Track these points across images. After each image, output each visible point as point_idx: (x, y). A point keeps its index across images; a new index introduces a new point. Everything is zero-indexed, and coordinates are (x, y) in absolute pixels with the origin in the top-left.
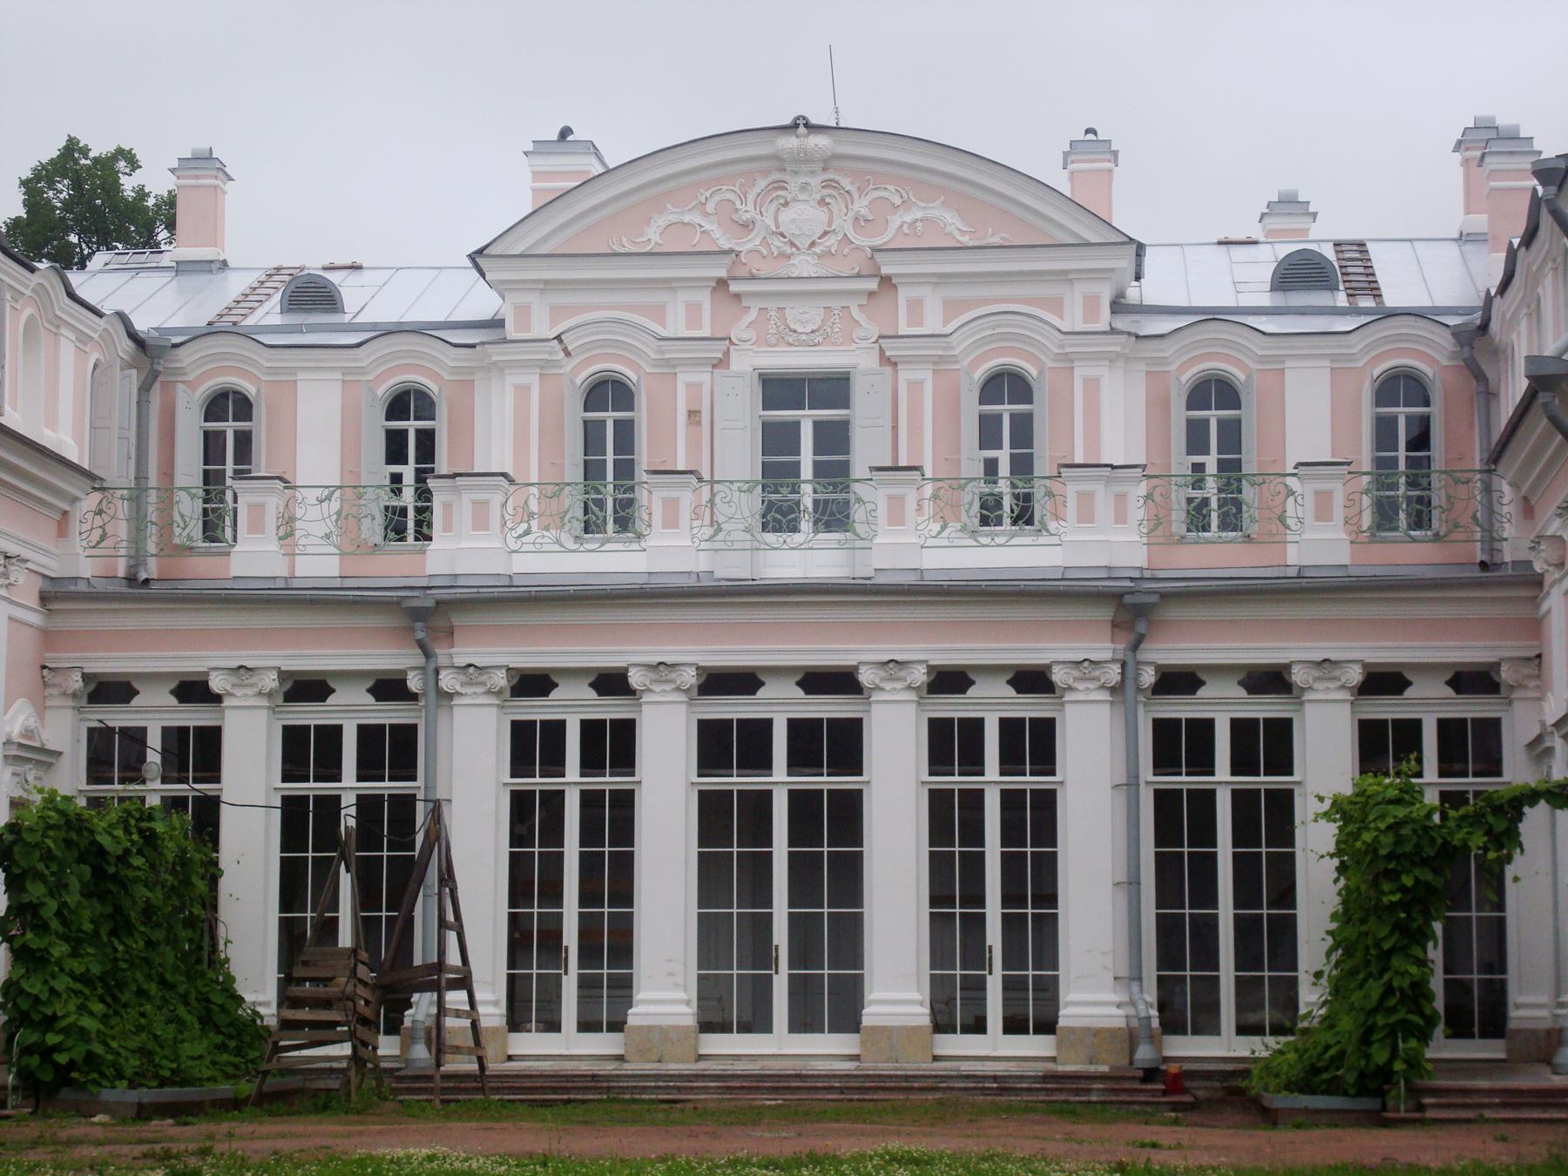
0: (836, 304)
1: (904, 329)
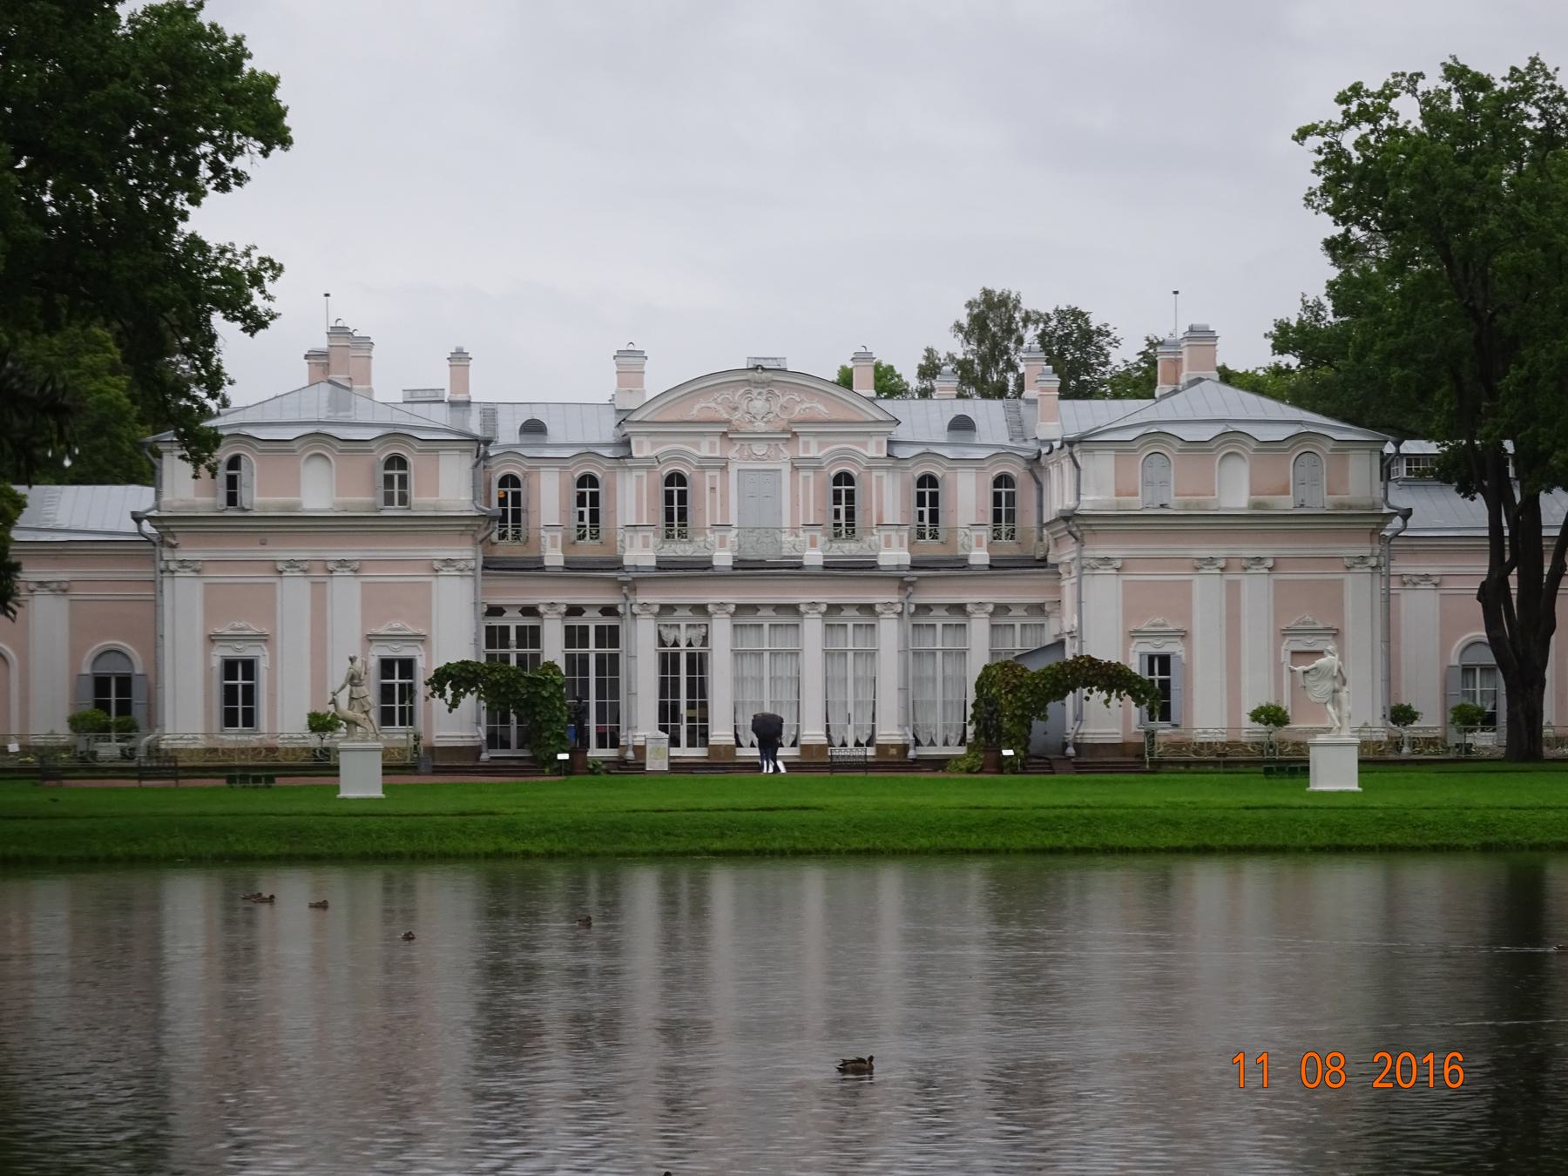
0: (772, 443)
1: (802, 455)
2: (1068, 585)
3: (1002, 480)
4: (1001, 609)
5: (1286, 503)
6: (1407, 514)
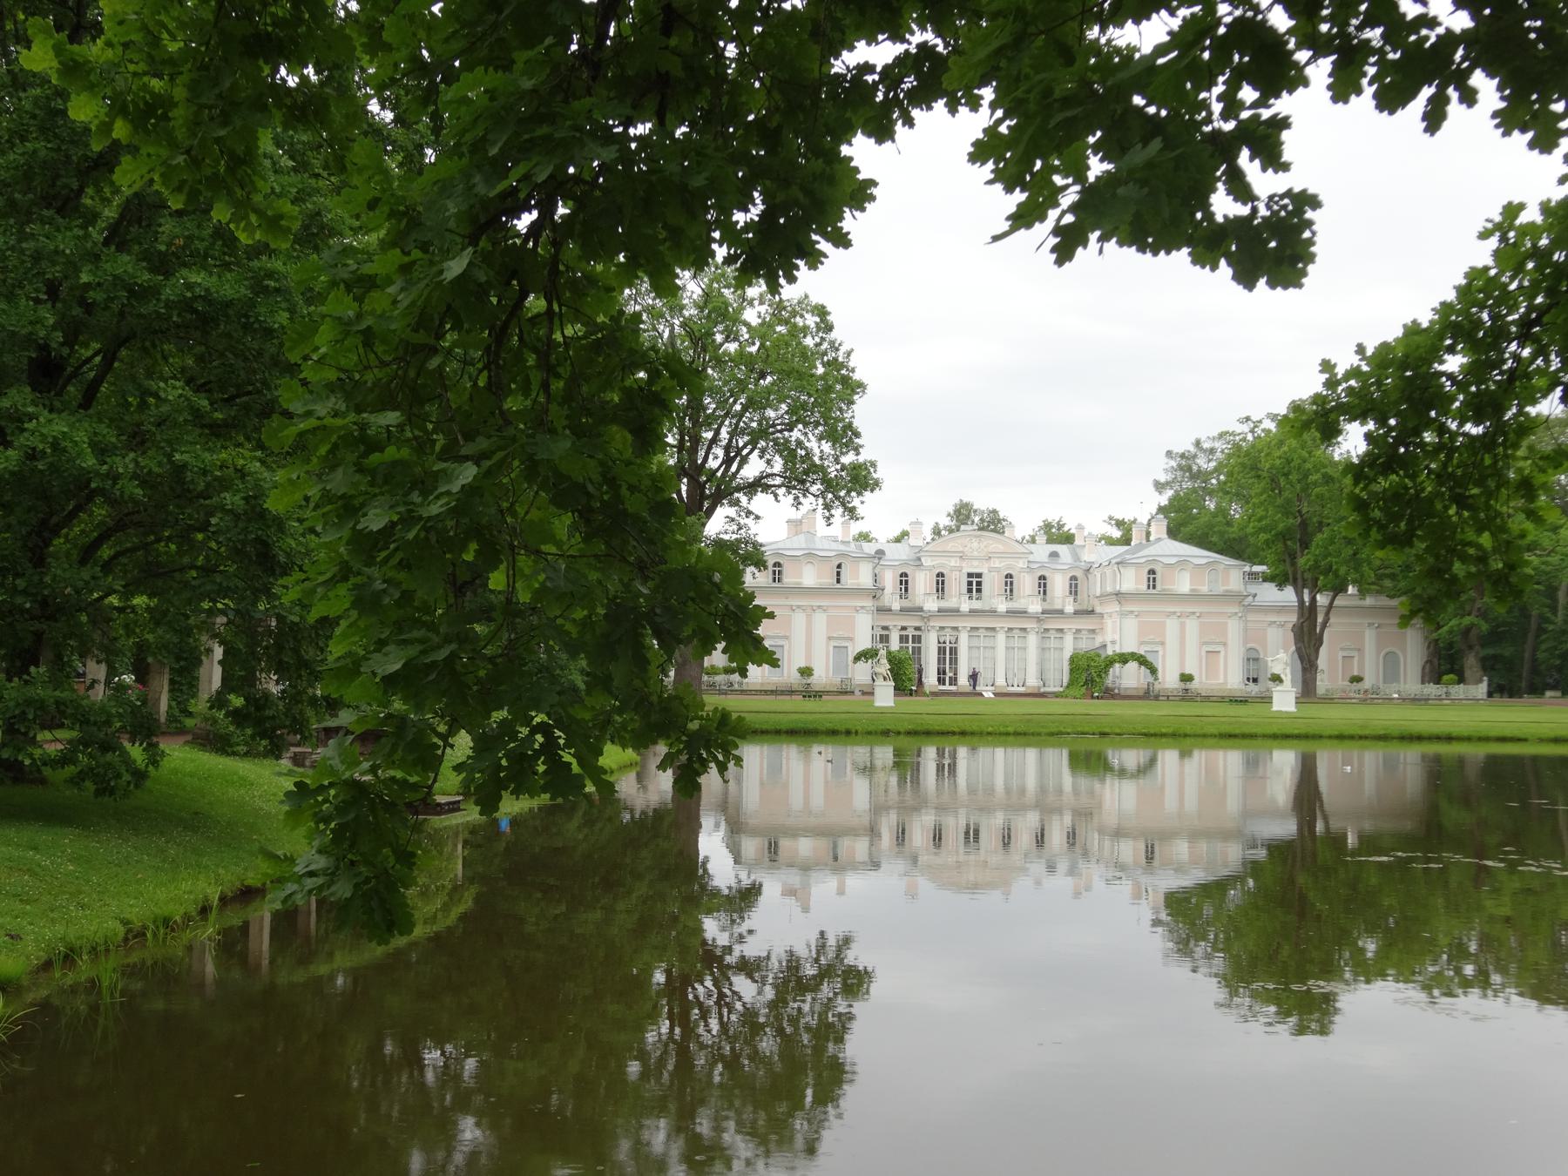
2: (1109, 623)
3: (1074, 578)
4: (1078, 631)
5: (1204, 589)
6: (1255, 596)
